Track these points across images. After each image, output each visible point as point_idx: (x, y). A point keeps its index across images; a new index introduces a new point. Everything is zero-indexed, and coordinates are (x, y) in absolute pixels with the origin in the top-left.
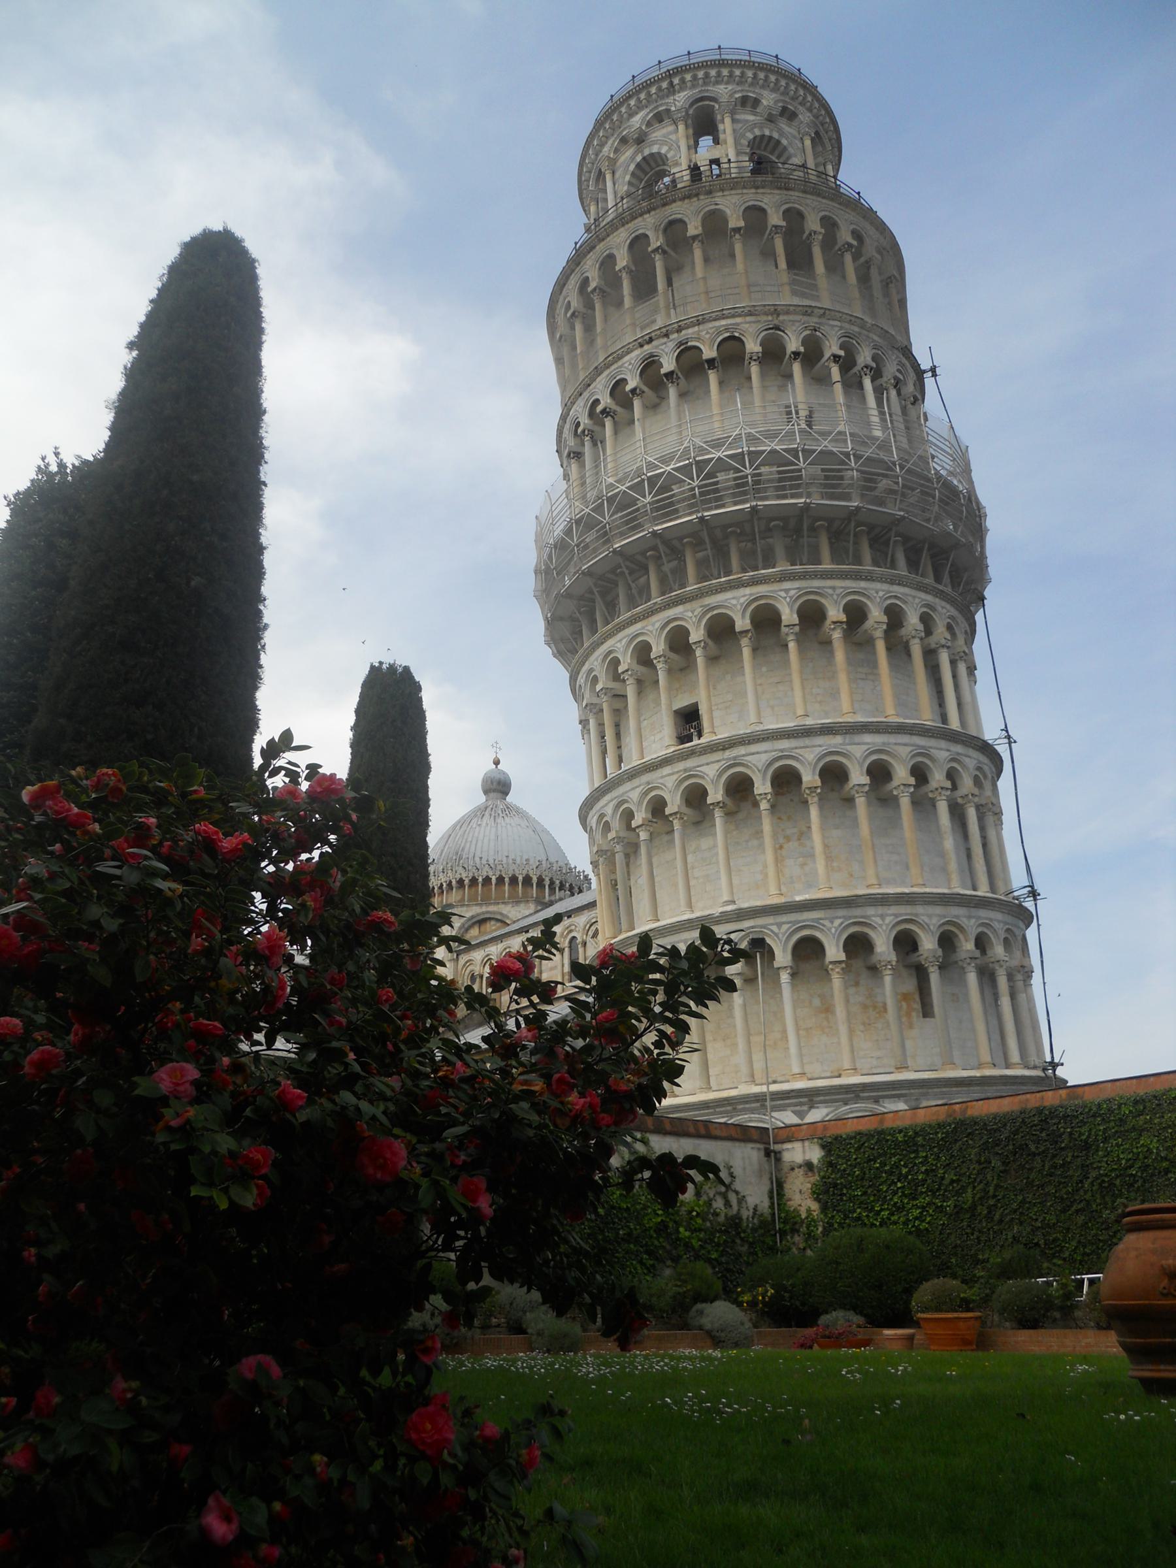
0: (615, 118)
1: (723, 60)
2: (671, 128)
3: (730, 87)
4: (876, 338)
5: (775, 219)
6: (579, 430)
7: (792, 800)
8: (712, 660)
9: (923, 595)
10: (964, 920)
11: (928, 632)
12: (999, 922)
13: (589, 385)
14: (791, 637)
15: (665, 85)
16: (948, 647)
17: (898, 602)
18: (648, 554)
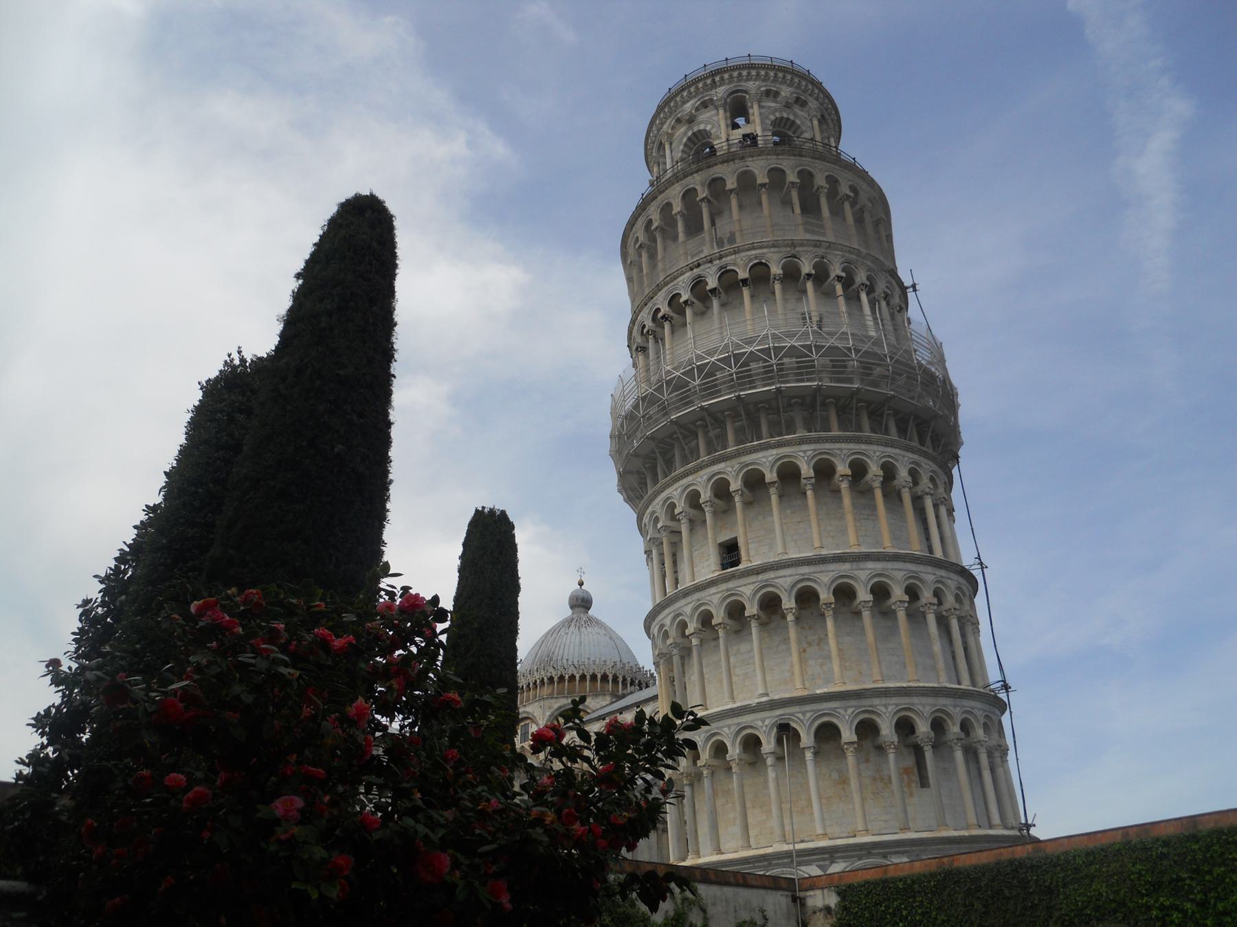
0: (672, 104)
1: (752, 64)
2: (714, 112)
3: (757, 83)
4: (869, 263)
5: (792, 177)
6: (645, 331)
7: (812, 614)
8: (748, 504)
9: (910, 455)
10: (951, 708)
11: (916, 482)
12: (979, 709)
13: (652, 298)
14: (809, 487)
15: (709, 81)
16: (931, 495)
17: (890, 460)
18: (698, 423)
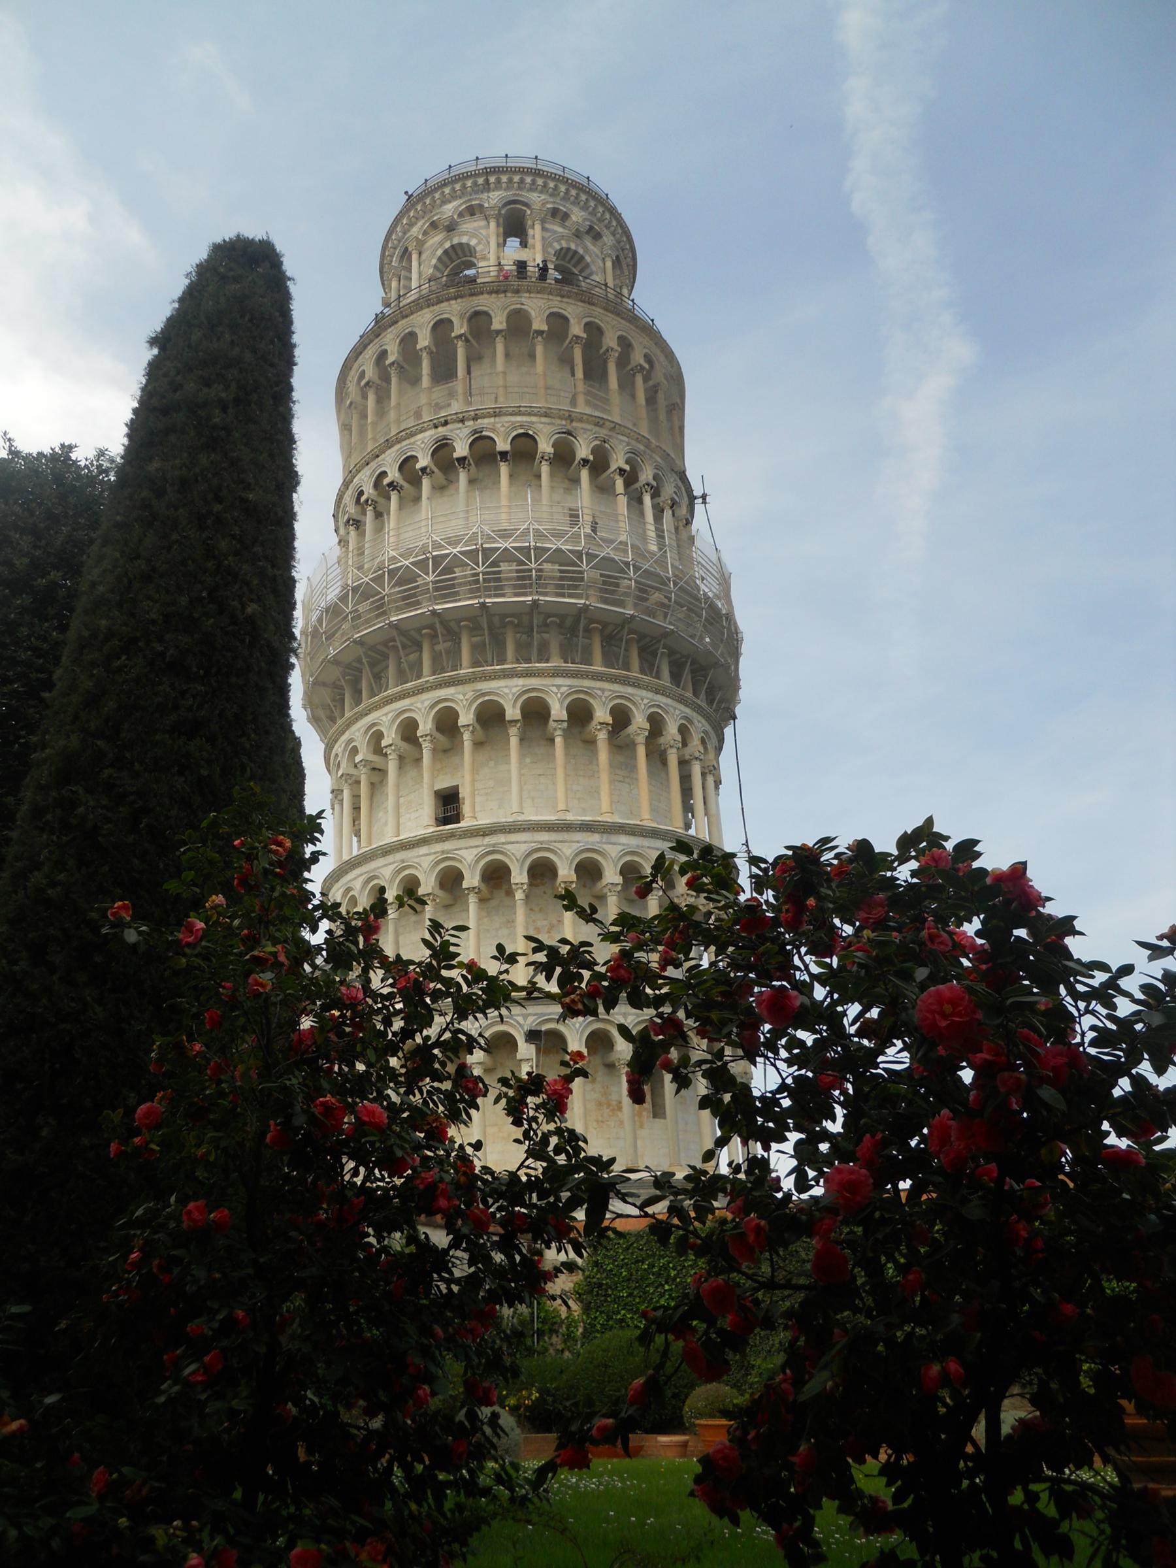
0: (428, 201)
2: (483, 223)
3: (543, 197)
4: (658, 459)
5: (576, 329)
6: (363, 499)
7: (545, 893)
8: (478, 745)
9: (682, 707)
11: (685, 744)
13: (378, 456)
14: (559, 732)
15: (481, 181)
16: (701, 760)
17: (660, 711)
18: (424, 631)
